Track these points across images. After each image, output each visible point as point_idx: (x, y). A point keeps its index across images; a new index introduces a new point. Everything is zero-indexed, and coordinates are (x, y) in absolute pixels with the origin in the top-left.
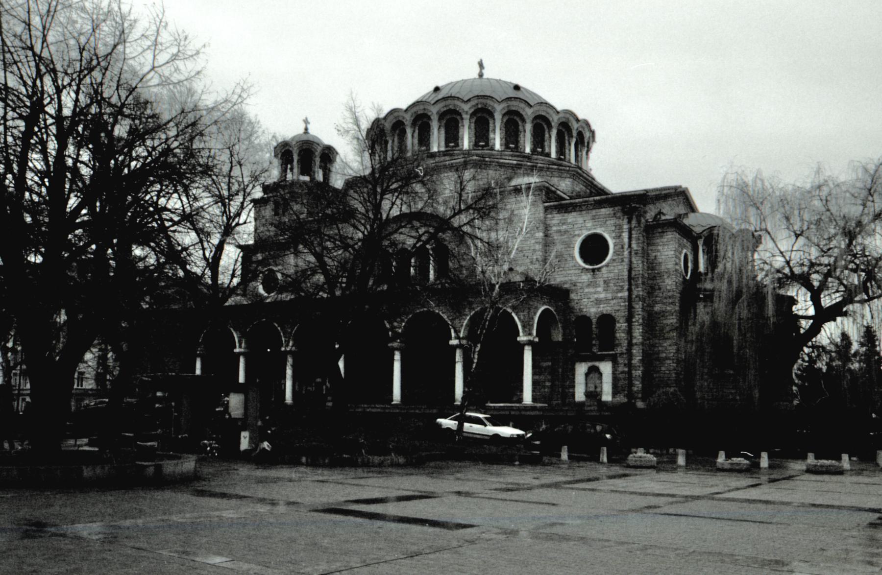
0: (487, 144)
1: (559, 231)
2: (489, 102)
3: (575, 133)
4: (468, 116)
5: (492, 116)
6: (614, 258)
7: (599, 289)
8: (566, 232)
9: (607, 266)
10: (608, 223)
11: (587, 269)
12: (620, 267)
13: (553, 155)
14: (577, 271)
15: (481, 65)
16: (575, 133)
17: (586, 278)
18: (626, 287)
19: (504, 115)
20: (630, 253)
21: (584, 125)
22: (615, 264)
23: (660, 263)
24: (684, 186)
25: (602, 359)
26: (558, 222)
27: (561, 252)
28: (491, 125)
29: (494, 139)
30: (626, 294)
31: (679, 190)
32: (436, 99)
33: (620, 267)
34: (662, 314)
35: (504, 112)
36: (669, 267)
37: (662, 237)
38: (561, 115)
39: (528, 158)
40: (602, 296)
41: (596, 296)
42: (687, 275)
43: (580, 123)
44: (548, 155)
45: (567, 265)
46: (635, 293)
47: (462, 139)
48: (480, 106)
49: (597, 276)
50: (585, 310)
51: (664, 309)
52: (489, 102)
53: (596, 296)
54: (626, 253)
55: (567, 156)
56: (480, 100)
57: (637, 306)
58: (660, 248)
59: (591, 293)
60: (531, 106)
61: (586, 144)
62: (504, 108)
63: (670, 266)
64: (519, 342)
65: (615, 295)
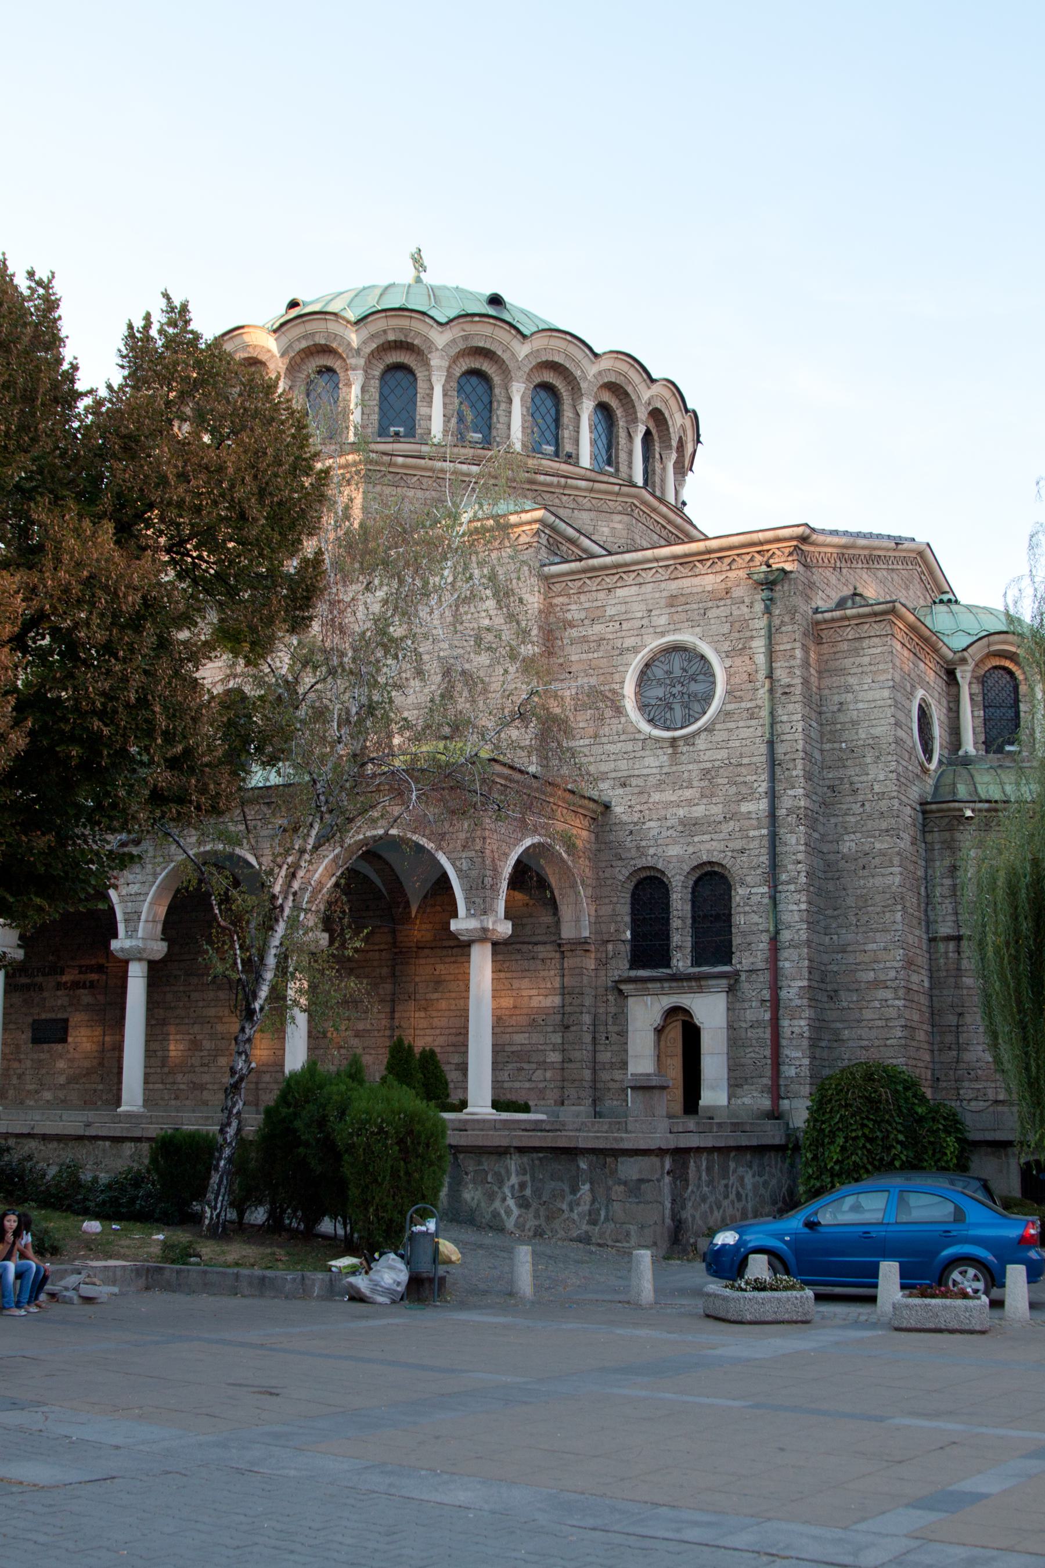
0: (411, 432)
1: (584, 640)
2: (417, 325)
3: (642, 413)
4: (362, 362)
5: (426, 364)
6: (729, 707)
9: (708, 729)
10: (710, 614)
11: (657, 740)
12: (745, 733)
13: (585, 461)
14: (629, 746)
16: (642, 413)
17: (654, 762)
18: (764, 787)
19: (455, 360)
20: (771, 691)
21: (667, 394)
22: (732, 725)
23: (854, 723)
24: (921, 538)
25: (695, 982)
26: (583, 615)
28: (421, 385)
29: (430, 418)
30: (764, 805)
31: (907, 545)
33: (745, 733)
35: (454, 351)
36: (877, 731)
37: (856, 652)
38: (604, 364)
40: (699, 811)
42: (929, 760)
43: (656, 389)
44: (572, 458)
45: (606, 730)
46: (786, 803)
49: (684, 758)
50: (652, 851)
51: (866, 848)
52: (417, 325)
53: (681, 812)
54: (763, 693)
55: (623, 468)
56: (394, 322)
57: (792, 839)
58: (852, 680)
59: (668, 805)
60: (524, 337)
61: (674, 443)
62: (453, 341)
63: (883, 729)
64: (453, 936)
65: (733, 807)
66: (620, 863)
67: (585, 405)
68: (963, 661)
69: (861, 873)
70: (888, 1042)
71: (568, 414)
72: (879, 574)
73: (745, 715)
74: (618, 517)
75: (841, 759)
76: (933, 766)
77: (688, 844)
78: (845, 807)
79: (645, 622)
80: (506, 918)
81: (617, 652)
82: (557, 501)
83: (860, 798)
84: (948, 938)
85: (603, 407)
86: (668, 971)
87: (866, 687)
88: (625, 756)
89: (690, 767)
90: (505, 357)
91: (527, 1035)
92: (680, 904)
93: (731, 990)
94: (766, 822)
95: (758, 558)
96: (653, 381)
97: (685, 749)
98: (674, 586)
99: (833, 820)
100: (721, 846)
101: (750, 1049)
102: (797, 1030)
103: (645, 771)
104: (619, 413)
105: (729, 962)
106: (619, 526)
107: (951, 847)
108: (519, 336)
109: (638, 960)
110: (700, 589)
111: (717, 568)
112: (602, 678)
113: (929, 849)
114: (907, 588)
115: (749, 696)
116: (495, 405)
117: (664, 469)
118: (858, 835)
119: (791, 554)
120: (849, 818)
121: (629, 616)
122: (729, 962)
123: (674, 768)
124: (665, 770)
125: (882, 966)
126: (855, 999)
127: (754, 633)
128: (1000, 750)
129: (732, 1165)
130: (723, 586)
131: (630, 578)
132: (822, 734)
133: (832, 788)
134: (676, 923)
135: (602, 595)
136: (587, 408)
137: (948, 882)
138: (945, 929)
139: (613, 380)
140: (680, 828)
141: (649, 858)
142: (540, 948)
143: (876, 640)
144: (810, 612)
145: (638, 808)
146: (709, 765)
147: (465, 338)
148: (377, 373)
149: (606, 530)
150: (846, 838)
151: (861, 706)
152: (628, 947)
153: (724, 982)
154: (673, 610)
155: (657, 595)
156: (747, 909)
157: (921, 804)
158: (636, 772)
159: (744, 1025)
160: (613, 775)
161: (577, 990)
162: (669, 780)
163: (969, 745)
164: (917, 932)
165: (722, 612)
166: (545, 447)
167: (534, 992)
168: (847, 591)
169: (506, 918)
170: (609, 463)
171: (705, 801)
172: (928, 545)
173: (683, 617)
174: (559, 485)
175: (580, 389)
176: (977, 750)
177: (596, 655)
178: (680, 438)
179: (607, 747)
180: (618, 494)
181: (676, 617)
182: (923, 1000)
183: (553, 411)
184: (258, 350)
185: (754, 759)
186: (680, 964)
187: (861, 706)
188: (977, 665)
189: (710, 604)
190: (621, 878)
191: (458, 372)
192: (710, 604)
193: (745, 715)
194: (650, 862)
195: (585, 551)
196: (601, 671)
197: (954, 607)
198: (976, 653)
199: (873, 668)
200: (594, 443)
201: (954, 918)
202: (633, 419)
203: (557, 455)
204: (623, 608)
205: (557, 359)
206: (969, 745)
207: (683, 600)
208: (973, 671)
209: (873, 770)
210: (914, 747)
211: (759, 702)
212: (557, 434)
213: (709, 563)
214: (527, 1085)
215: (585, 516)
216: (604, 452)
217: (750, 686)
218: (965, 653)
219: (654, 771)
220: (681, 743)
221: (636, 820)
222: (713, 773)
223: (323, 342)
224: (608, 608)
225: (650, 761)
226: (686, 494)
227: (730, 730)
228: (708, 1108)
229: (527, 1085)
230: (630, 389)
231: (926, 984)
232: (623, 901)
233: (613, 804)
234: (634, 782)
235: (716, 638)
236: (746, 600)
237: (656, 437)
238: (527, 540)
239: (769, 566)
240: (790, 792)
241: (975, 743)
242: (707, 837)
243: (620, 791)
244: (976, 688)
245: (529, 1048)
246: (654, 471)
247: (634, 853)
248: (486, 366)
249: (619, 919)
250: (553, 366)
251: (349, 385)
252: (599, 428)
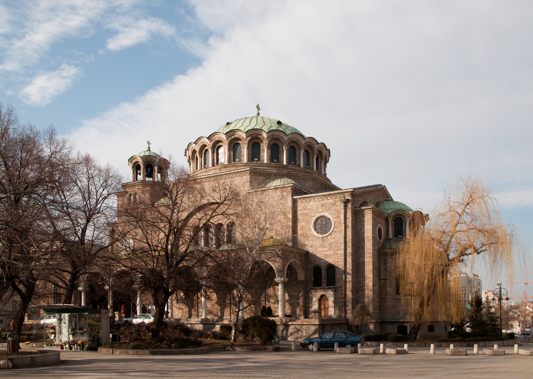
1: (302, 214)
3: (316, 152)
8: (306, 214)
12: (339, 236)
13: (302, 166)
14: (313, 238)
15: (258, 108)
16: (316, 152)
21: (322, 146)
22: (336, 234)
26: (302, 208)
27: (303, 227)
30: (343, 252)
32: (228, 130)
33: (339, 236)
38: (306, 140)
39: (285, 167)
40: (328, 253)
41: (324, 253)
42: (381, 240)
43: (319, 145)
44: (299, 166)
47: (244, 156)
48: (254, 136)
50: (318, 261)
53: (324, 253)
55: (311, 166)
60: (287, 135)
61: (324, 158)
65: (336, 252)
67: (302, 151)
68: (390, 216)
71: (297, 153)
72: (372, 195)
73: (339, 232)
74: (310, 181)
75: (360, 241)
76: (381, 241)
79: (316, 210)
80: (287, 277)
81: (310, 217)
84: (384, 279)
85: (306, 151)
89: (326, 243)
90: (282, 140)
92: (324, 273)
93: (335, 291)
94: (343, 255)
95: (342, 196)
96: (318, 144)
97: (325, 239)
98: (323, 202)
99: (358, 254)
103: (316, 244)
104: (310, 152)
105: (335, 285)
106: (310, 183)
107: (385, 259)
108: (285, 135)
110: (329, 203)
111: (333, 198)
112: (306, 223)
113: (379, 259)
114: (379, 197)
115: (340, 227)
116: (280, 152)
117: (321, 165)
119: (349, 195)
120: (361, 254)
121: (313, 209)
122: (335, 285)
123: (323, 243)
127: (341, 213)
128: (397, 237)
129: (334, 327)
130: (334, 202)
131: (312, 200)
132: (356, 235)
133: (358, 247)
134: (323, 277)
135: (306, 203)
136: (302, 152)
137: (383, 267)
138: (382, 277)
140: (324, 257)
142: (293, 282)
143: (369, 214)
144: (354, 208)
146: (330, 243)
147: (272, 135)
148: (251, 145)
149: (307, 185)
152: (313, 282)
153: (333, 290)
154: (323, 207)
155: (319, 204)
158: (314, 244)
159: (338, 298)
160: (309, 245)
162: (323, 246)
163: (391, 236)
164: (376, 278)
165: (334, 208)
166: (292, 162)
167: (292, 292)
168: (363, 201)
169: (287, 277)
170: (308, 165)
172: (384, 186)
173: (325, 209)
174: (296, 174)
175: (300, 147)
176: (392, 237)
178: (325, 156)
180: (310, 176)
181: (323, 209)
182: (377, 292)
183: (294, 153)
184: (221, 138)
185: (340, 242)
188: (393, 217)
189: (331, 206)
191: (271, 144)
192: (331, 206)
193: (339, 232)
194: (317, 264)
195: (302, 191)
197: (390, 202)
198: (393, 214)
199: (368, 221)
200: (304, 160)
202: (314, 154)
203: (295, 164)
205: (295, 140)
206: (391, 236)
207: (325, 205)
208: (392, 219)
211: (342, 229)
212: (295, 159)
213: (331, 197)
215: (302, 181)
216: (306, 162)
217: (340, 225)
220: (324, 238)
223: (237, 137)
224: (308, 207)
225: (318, 242)
226: (327, 172)
227: (335, 235)
230: (313, 146)
231: (378, 289)
234: (314, 246)
236: (340, 206)
237: (319, 157)
238: (289, 190)
239: (344, 198)
241: (392, 235)
242: (330, 258)
243: (311, 248)
244: (393, 222)
246: (319, 165)
248: (277, 143)
250: (294, 142)
251: (244, 148)
252: (305, 156)
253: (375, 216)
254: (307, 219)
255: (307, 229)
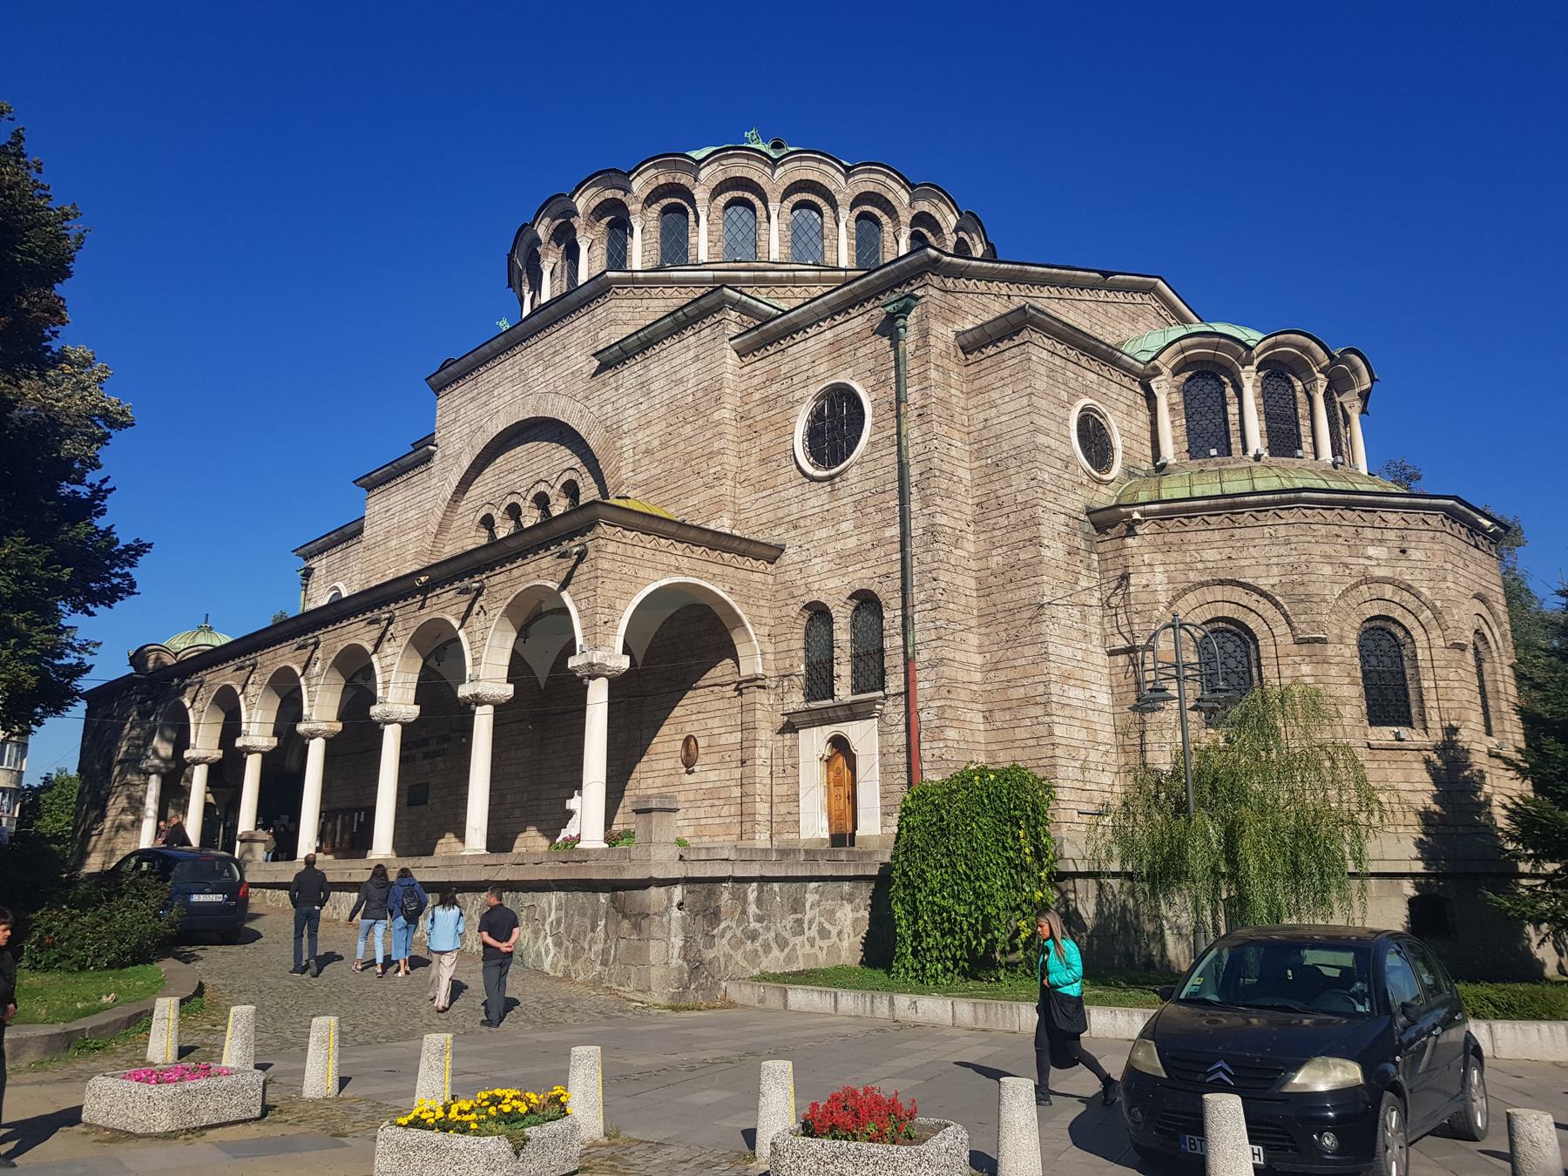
6: (874, 439)
7: (845, 527)
9: (859, 464)
10: (859, 354)
34: (1009, 575)
40: (851, 543)
41: (839, 546)
45: (780, 480)
50: (816, 586)
53: (839, 546)
65: (879, 534)
66: (792, 601)
68: (1157, 372)
69: (1008, 587)
70: (1040, 763)
77: (844, 575)
78: (991, 522)
79: (810, 373)
81: (790, 405)
82: (789, 293)
83: (1006, 511)
86: (830, 701)
87: (1007, 399)
88: (796, 500)
91: (717, 772)
100: (867, 573)
101: (898, 775)
102: (936, 752)
109: (810, 695)
110: (851, 333)
118: (1005, 548)
123: (832, 505)
124: (826, 507)
125: (1030, 681)
126: (1008, 718)
131: (798, 338)
139: (872, 190)
140: (838, 561)
141: (814, 593)
145: (807, 546)
146: (859, 497)
150: (994, 552)
151: (1003, 418)
156: (892, 631)
157: (1088, 514)
161: (751, 725)
162: (828, 517)
171: (856, 532)
177: (774, 412)
179: (782, 494)
186: (841, 693)
187: (1003, 418)
189: (859, 345)
190: (794, 615)
192: (859, 345)
193: (888, 443)
194: (814, 597)
196: (778, 425)
201: (1128, 629)
204: (793, 365)
206: (1169, 452)
209: (1015, 481)
210: (1074, 456)
214: (718, 821)
218: (1156, 362)
219: (817, 510)
221: (804, 558)
222: (863, 503)
227: (875, 460)
228: (863, 838)
229: (718, 821)
232: (797, 637)
233: (788, 546)
235: (864, 376)
240: (925, 511)
242: (859, 566)
243: (793, 533)
245: (718, 784)
247: (803, 590)
249: (793, 654)
253: (1058, 361)
254: (779, 418)
255: (779, 457)
